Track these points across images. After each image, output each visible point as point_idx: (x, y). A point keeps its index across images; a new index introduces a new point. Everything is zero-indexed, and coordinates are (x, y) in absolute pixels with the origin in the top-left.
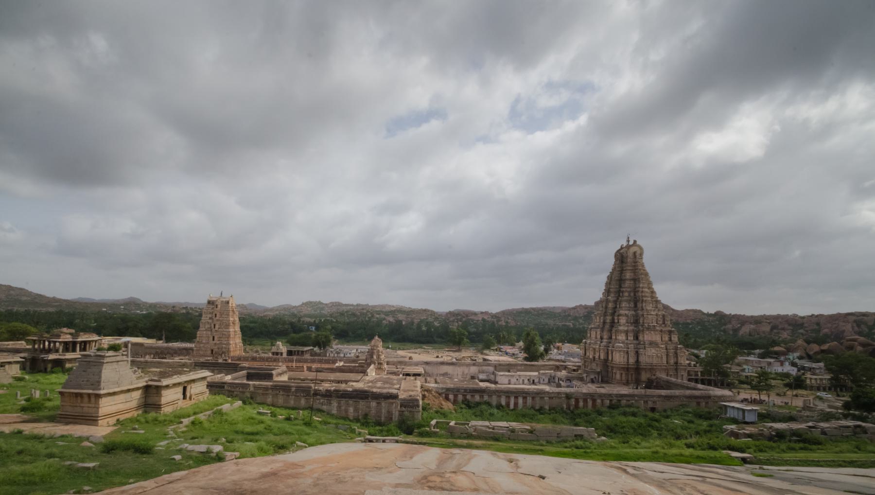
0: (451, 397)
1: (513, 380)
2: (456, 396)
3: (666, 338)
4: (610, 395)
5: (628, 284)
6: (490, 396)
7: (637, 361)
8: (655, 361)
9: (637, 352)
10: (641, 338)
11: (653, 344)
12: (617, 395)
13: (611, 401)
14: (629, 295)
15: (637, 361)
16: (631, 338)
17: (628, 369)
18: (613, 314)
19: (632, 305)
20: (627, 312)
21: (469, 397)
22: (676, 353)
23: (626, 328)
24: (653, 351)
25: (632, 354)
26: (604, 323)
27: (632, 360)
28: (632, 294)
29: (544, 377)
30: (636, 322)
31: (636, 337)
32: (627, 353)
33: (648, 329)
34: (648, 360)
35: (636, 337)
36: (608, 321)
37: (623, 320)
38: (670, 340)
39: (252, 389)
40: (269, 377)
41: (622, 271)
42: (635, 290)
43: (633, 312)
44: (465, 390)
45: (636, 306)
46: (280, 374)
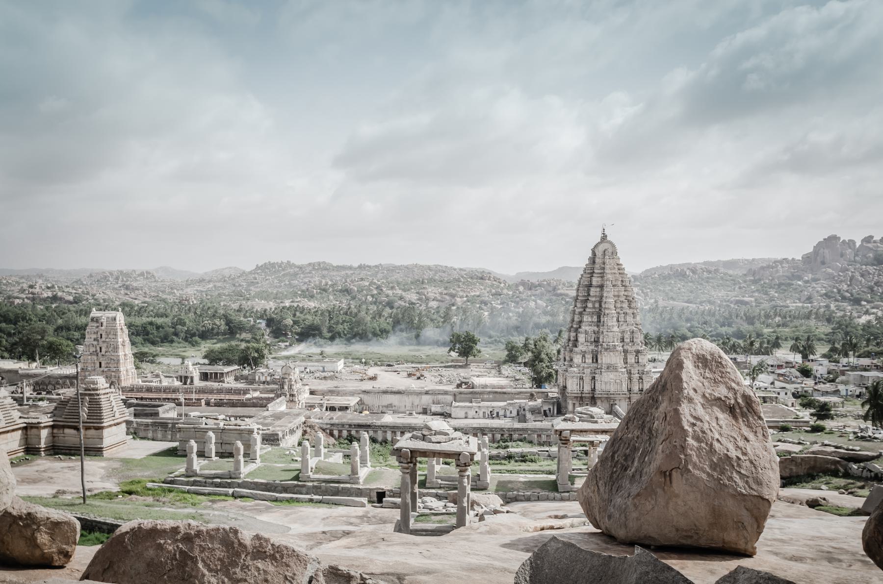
0: (336, 433)
1: (471, 413)
2: (340, 432)
3: (631, 359)
4: (502, 429)
5: (593, 291)
6: (375, 432)
7: (594, 390)
8: (612, 389)
9: (594, 378)
10: (599, 361)
11: (611, 368)
12: (509, 430)
13: (502, 435)
14: (594, 307)
15: (594, 390)
16: (589, 360)
17: (581, 398)
18: (576, 330)
19: (595, 319)
20: (587, 328)
21: (353, 433)
22: (641, 378)
23: (584, 349)
25: (587, 379)
26: (569, 340)
27: (587, 388)
28: (597, 305)
29: (511, 408)
30: (596, 341)
31: (595, 359)
32: (581, 379)
33: (606, 349)
34: (603, 387)
35: (595, 359)
36: (572, 339)
37: (581, 338)
39: (135, 425)
40: (157, 414)
41: (592, 274)
43: (596, 329)
44: (350, 425)
45: (599, 321)
46: (167, 411)
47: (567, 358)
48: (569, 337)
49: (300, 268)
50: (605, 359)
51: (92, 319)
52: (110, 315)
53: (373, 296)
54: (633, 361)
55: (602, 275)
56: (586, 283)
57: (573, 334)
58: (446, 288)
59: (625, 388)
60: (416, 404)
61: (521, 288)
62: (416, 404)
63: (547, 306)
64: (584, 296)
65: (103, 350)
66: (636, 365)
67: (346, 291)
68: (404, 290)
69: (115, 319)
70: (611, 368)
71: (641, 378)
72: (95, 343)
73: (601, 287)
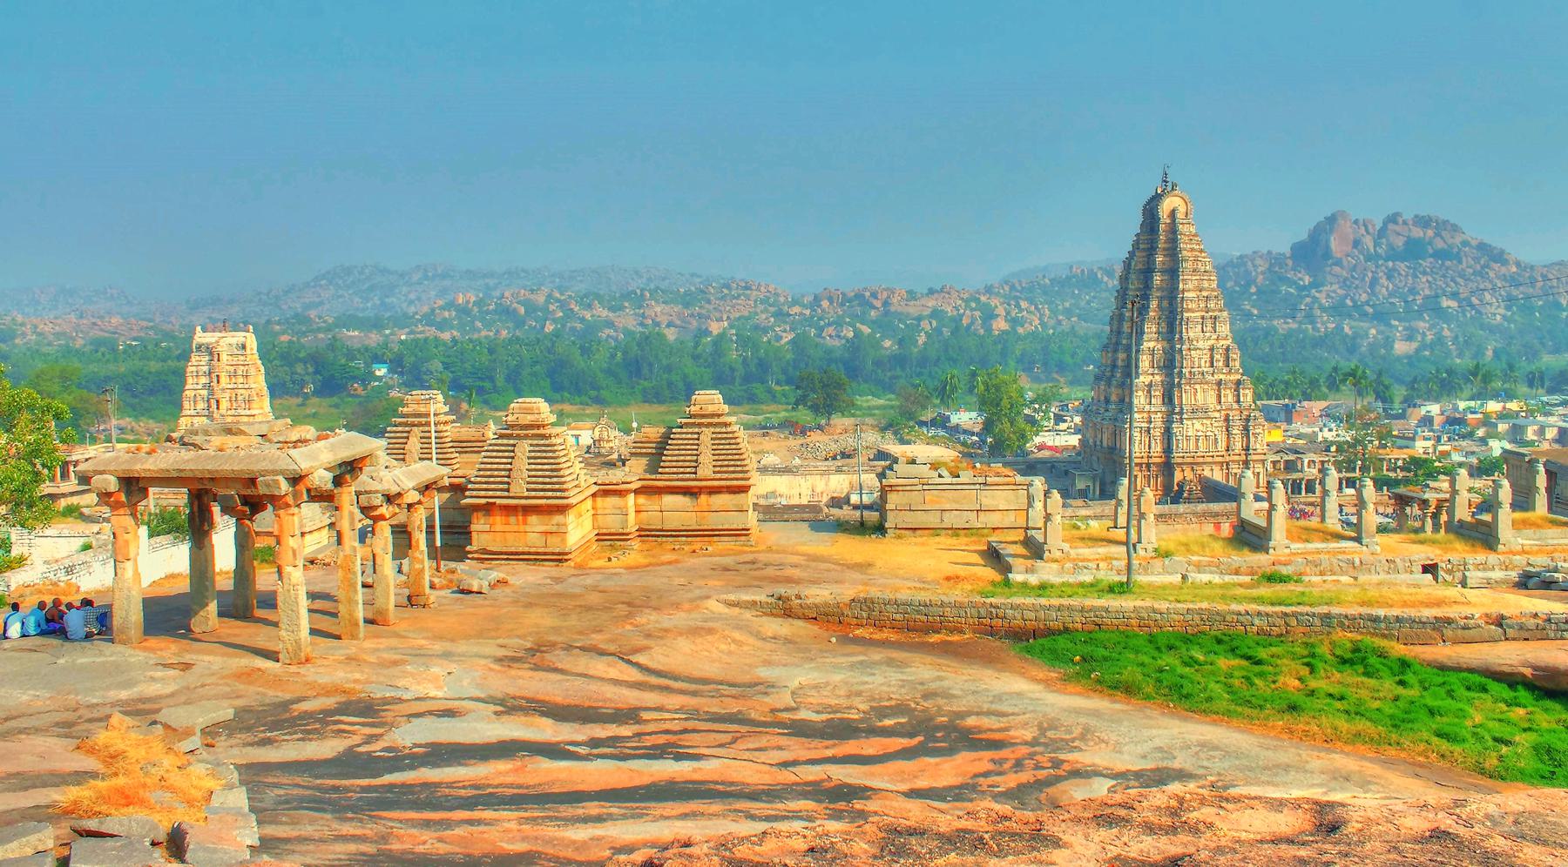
3: (1228, 397)
5: (1157, 279)
7: (1168, 450)
11: (1200, 412)
15: (1168, 450)
17: (1148, 465)
22: (1246, 429)
24: (1198, 425)
26: (1114, 366)
27: (1157, 448)
28: (1165, 304)
31: (1168, 398)
36: (1120, 363)
37: (1145, 362)
38: (1238, 401)
41: (1152, 250)
42: (1172, 297)
43: (1165, 344)
47: (1113, 398)
48: (1114, 360)
49: (402, 276)
50: (1189, 397)
51: (199, 347)
52: (234, 341)
53: (555, 321)
54: (1230, 398)
55: (1173, 252)
56: (1140, 266)
57: (1121, 356)
58: (687, 305)
59: (1222, 445)
60: (819, 490)
61: (825, 304)
62: (819, 490)
63: (874, 332)
64: (1138, 289)
65: (224, 404)
66: (1235, 406)
67: (506, 312)
68: (612, 309)
69: (244, 347)
70: (1200, 412)
71: (1246, 429)
72: (205, 392)
73: (1173, 272)
